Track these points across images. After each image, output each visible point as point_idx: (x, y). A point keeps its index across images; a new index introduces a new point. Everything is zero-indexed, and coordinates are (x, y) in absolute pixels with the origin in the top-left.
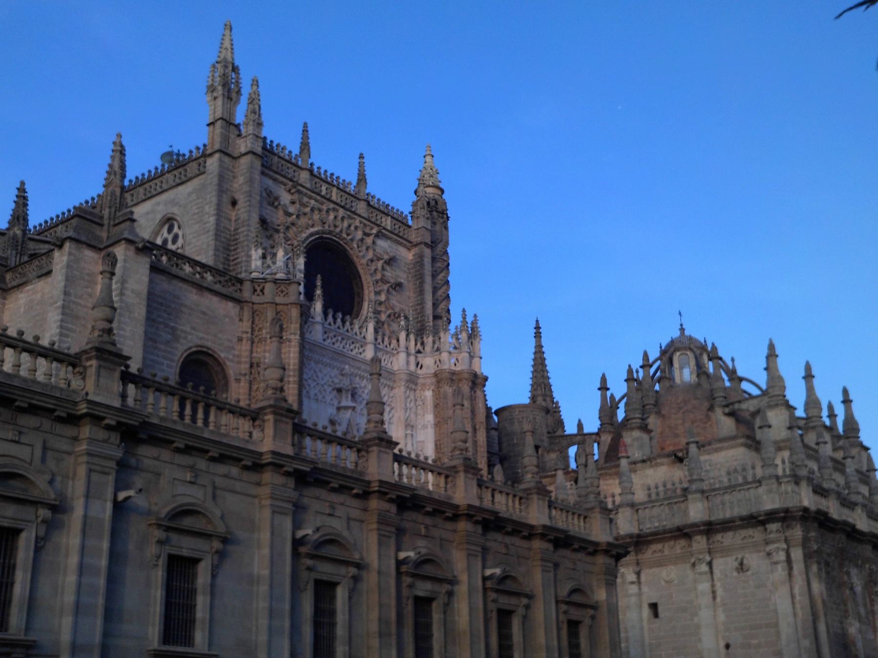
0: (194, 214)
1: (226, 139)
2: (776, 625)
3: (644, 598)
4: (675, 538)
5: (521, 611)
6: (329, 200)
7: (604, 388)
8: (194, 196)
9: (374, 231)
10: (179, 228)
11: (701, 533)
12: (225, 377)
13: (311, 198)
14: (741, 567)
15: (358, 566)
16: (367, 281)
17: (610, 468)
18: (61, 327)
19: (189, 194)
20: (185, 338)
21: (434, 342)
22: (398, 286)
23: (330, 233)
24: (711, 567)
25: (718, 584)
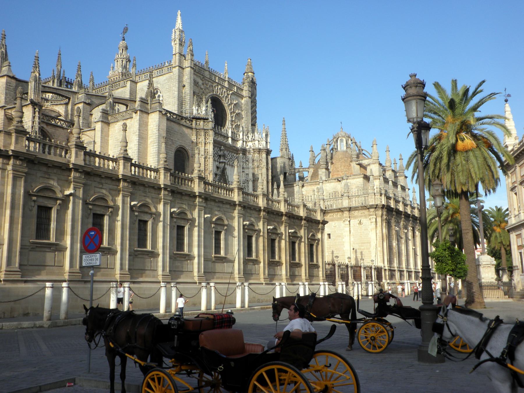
0: (167, 88)
2: (370, 243)
4: (338, 212)
8: (166, 81)
9: (231, 92)
10: (160, 93)
11: (347, 210)
12: (188, 156)
13: (209, 81)
14: (360, 223)
16: (228, 112)
17: (314, 182)
18: (139, 142)
19: (164, 80)
20: (176, 143)
21: (252, 136)
24: (350, 223)
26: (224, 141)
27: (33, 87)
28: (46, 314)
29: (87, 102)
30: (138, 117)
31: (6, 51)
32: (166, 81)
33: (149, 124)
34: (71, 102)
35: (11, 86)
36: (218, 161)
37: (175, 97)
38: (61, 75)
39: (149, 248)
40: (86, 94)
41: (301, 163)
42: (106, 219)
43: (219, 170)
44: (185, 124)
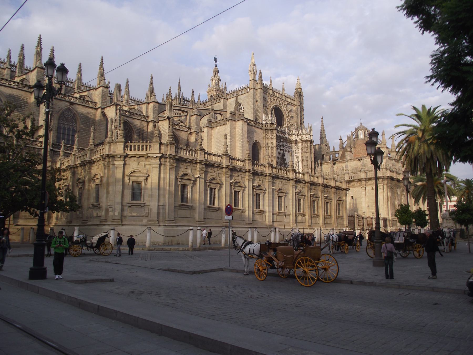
1: (254, 85)
3: (350, 195)
4: (357, 181)
5: (330, 202)
6: (277, 97)
7: (341, 139)
9: (287, 103)
11: (364, 180)
12: (261, 147)
15: (304, 196)
16: (285, 116)
17: (342, 161)
18: (231, 140)
19: (245, 97)
21: (301, 132)
22: (292, 117)
23: (277, 105)
24: (365, 189)
25: (367, 192)
26: (283, 136)
27: (169, 108)
28: (190, 244)
29: (199, 114)
30: (230, 124)
31: (153, 87)
32: (246, 98)
33: (236, 128)
34: (189, 115)
35: (156, 108)
36: (279, 149)
37: (251, 109)
38: (181, 96)
39: (240, 207)
40: (198, 109)
41: (334, 147)
42: (217, 191)
43: (280, 155)
44: (258, 126)
